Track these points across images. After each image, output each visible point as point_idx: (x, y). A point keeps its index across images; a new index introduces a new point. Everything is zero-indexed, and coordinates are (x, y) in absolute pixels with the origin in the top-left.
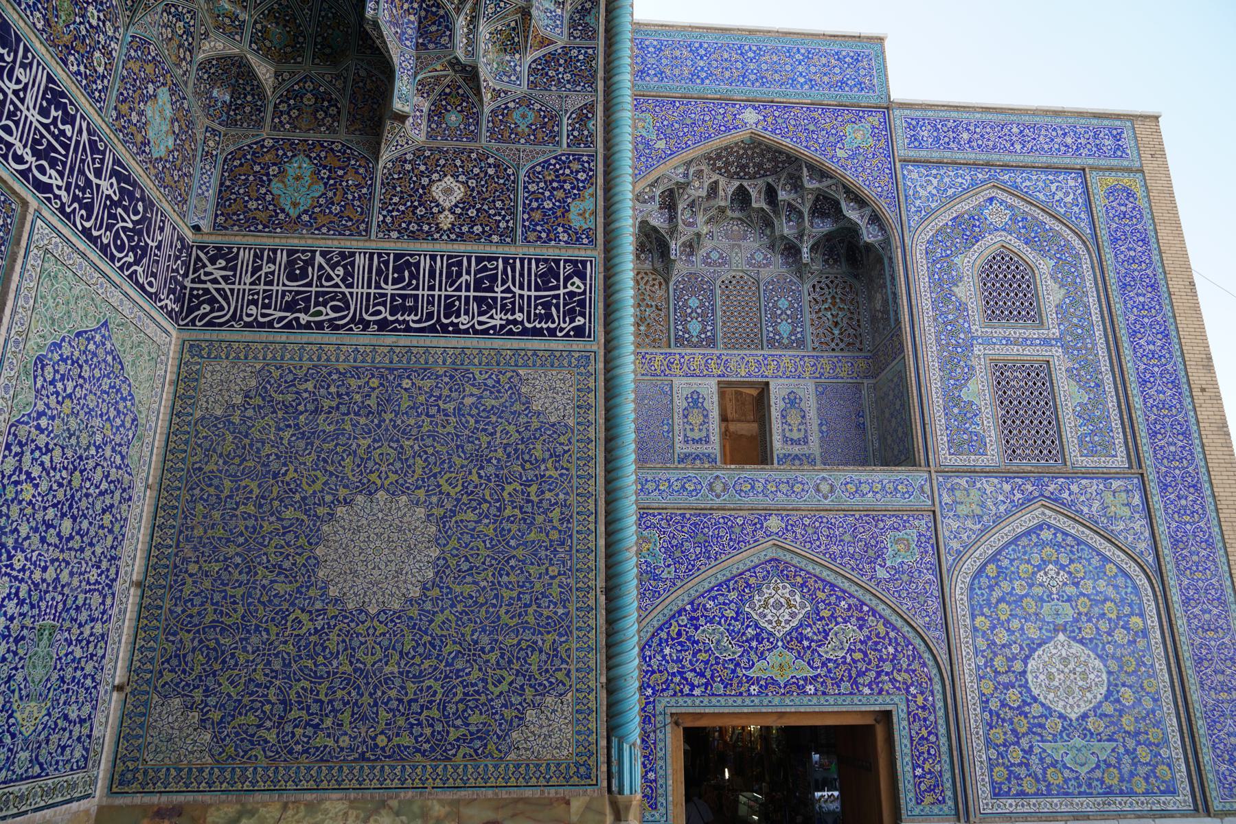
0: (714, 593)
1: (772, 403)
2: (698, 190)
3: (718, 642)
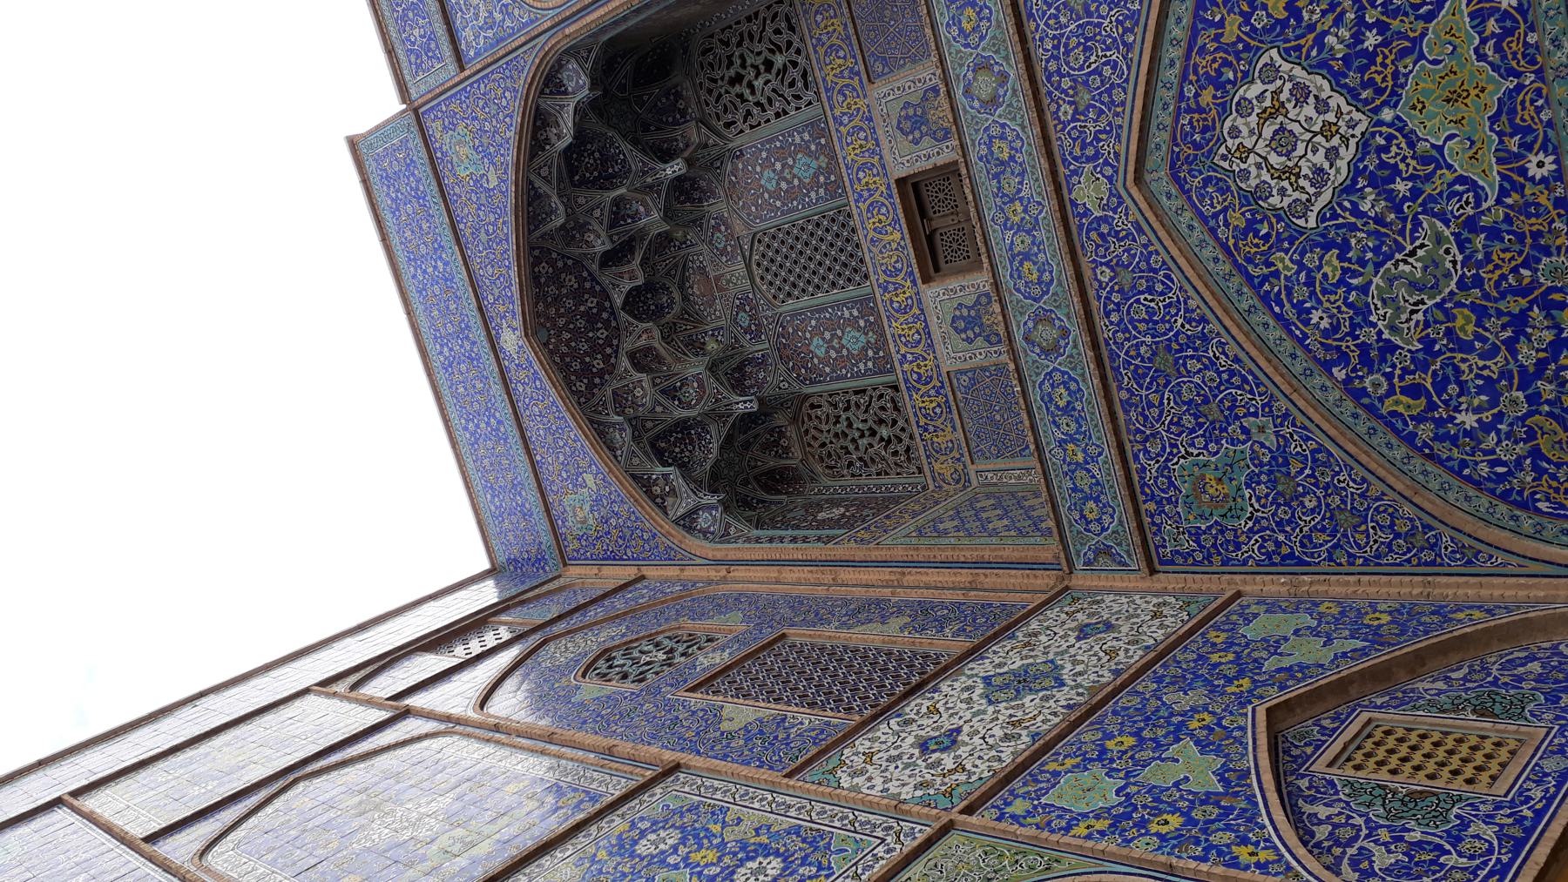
0: (1291, 314)
1: (928, 165)
2: (644, 389)
3: (1414, 286)
